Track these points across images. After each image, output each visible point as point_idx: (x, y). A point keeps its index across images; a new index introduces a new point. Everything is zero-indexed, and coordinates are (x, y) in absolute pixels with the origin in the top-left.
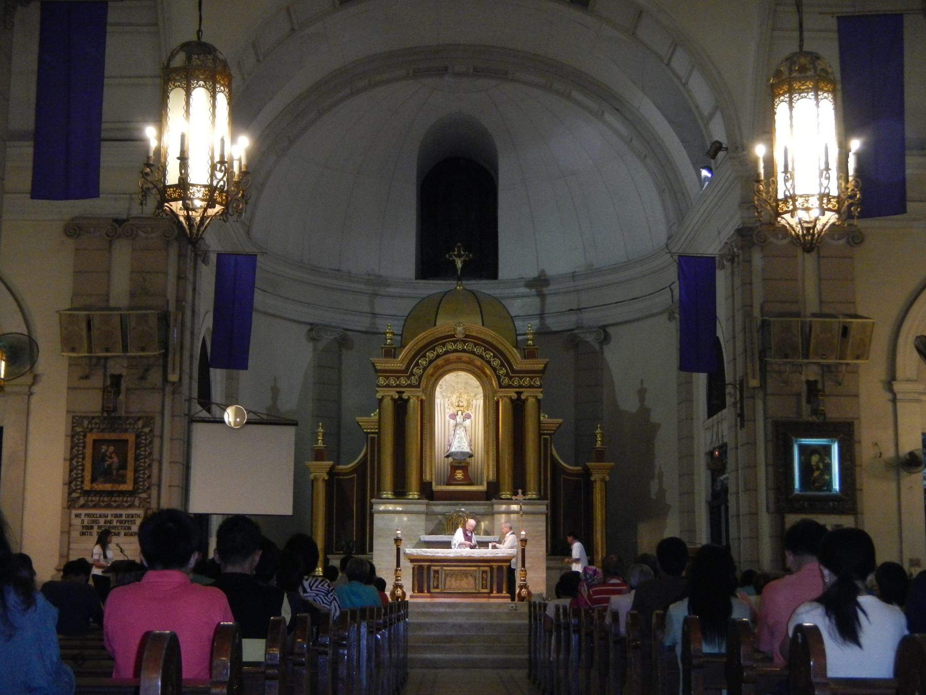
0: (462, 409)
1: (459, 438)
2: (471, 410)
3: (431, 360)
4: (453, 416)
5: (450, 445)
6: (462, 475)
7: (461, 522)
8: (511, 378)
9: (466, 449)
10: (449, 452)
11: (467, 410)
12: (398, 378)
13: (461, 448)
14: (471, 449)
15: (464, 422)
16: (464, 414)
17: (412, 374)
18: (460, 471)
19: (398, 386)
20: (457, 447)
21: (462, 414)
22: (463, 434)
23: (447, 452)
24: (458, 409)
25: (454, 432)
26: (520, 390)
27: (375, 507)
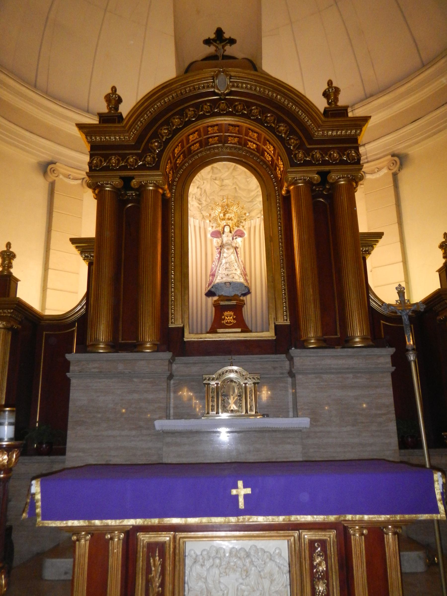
0: (230, 223)
1: (226, 263)
2: (243, 227)
4: (217, 234)
5: (213, 275)
6: (234, 319)
7: (234, 392)
8: (307, 152)
9: (240, 280)
10: (213, 284)
11: (238, 227)
13: (231, 276)
14: (246, 280)
15: (235, 240)
16: (233, 232)
17: (148, 150)
18: (232, 313)
19: (124, 168)
20: (224, 276)
21: (231, 232)
22: (233, 257)
23: (209, 286)
24: (224, 223)
25: (218, 255)
26: (327, 168)
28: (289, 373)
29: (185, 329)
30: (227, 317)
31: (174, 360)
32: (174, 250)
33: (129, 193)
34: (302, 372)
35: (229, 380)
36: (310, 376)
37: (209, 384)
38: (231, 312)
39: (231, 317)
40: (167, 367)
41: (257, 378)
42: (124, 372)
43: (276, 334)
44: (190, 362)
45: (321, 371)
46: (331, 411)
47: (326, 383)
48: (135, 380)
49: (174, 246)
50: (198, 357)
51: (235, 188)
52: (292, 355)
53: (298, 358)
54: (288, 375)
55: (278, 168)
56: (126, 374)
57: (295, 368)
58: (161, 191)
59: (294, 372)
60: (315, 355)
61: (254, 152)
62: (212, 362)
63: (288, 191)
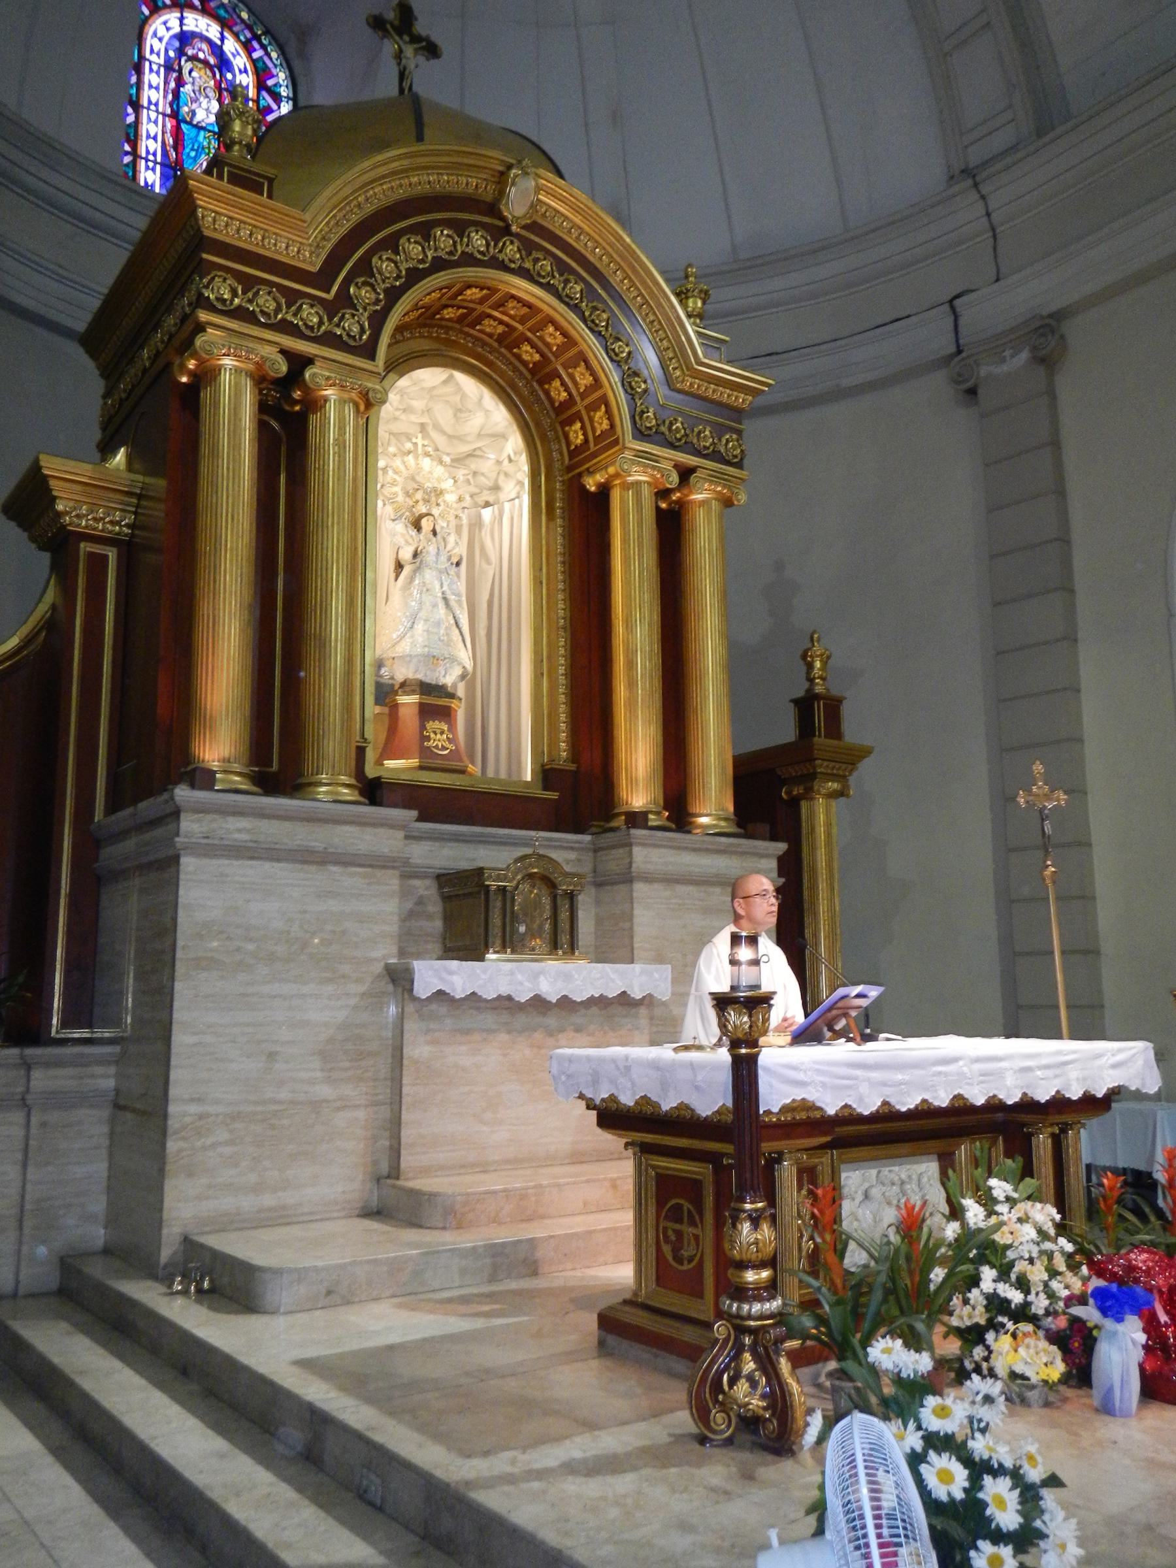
3: (416, 269)
12: (292, 297)
27: (190, 826)
38: (443, 723)
39: (445, 736)
61: (522, 368)
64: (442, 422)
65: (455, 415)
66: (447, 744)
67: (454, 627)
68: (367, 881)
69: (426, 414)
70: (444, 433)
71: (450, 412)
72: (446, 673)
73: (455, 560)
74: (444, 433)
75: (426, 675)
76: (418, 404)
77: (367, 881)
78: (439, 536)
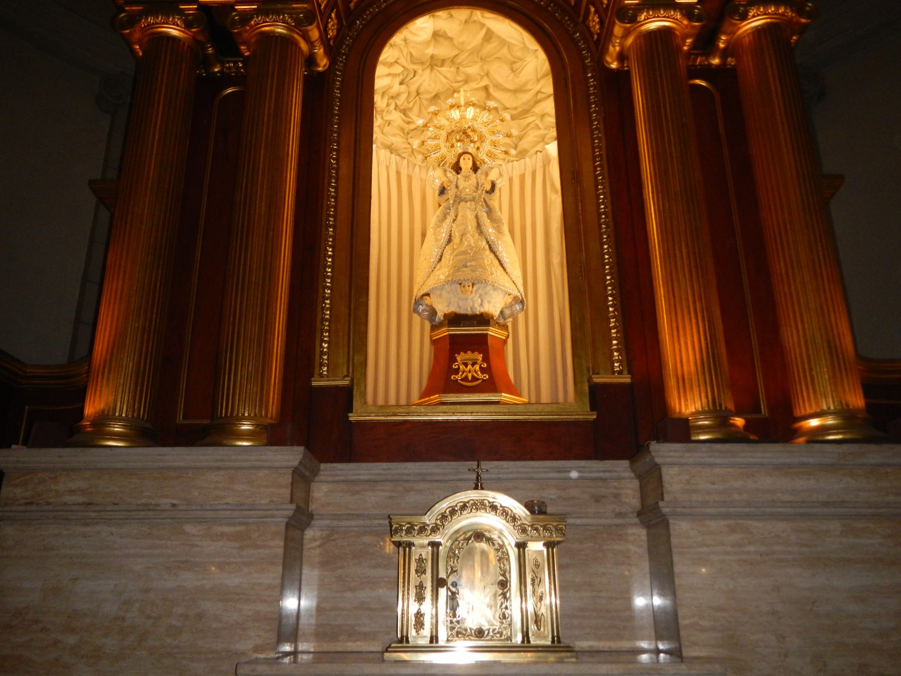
6: (482, 370)
28: (639, 514)
29: (355, 393)
30: (466, 365)
31: (315, 472)
32: (336, 198)
33: (228, 62)
34: (688, 511)
35: (469, 534)
36: (712, 524)
37: (410, 545)
38: (476, 353)
40: (287, 492)
41: (556, 527)
42: (158, 505)
43: (593, 408)
44: (361, 477)
45: (747, 510)
46: (784, 638)
47: (763, 549)
48: (189, 528)
49: (336, 188)
50: (384, 465)
51: (486, 88)
52: (658, 460)
53: (675, 470)
54: (637, 520)
55: (593, 9)
56: (163, 510)
57: (666, 497)
58: (303, 46)
59: (665, 510)
60: (726, 461)
62: (424, 478)
63: (622, 57)
64: (500, 80)
65: (513, 71)
66: (480, 376)
67: (488, 252)
68: (237, 545)
69: (485, 78)
70: (506, 90)
71: (506, 68)
72: (482, 301)
73: (488, 187)
74: (506, 90)
75: (460, 307)
76: (473, 70)
77: (237, 545)
78: (479, 172)
